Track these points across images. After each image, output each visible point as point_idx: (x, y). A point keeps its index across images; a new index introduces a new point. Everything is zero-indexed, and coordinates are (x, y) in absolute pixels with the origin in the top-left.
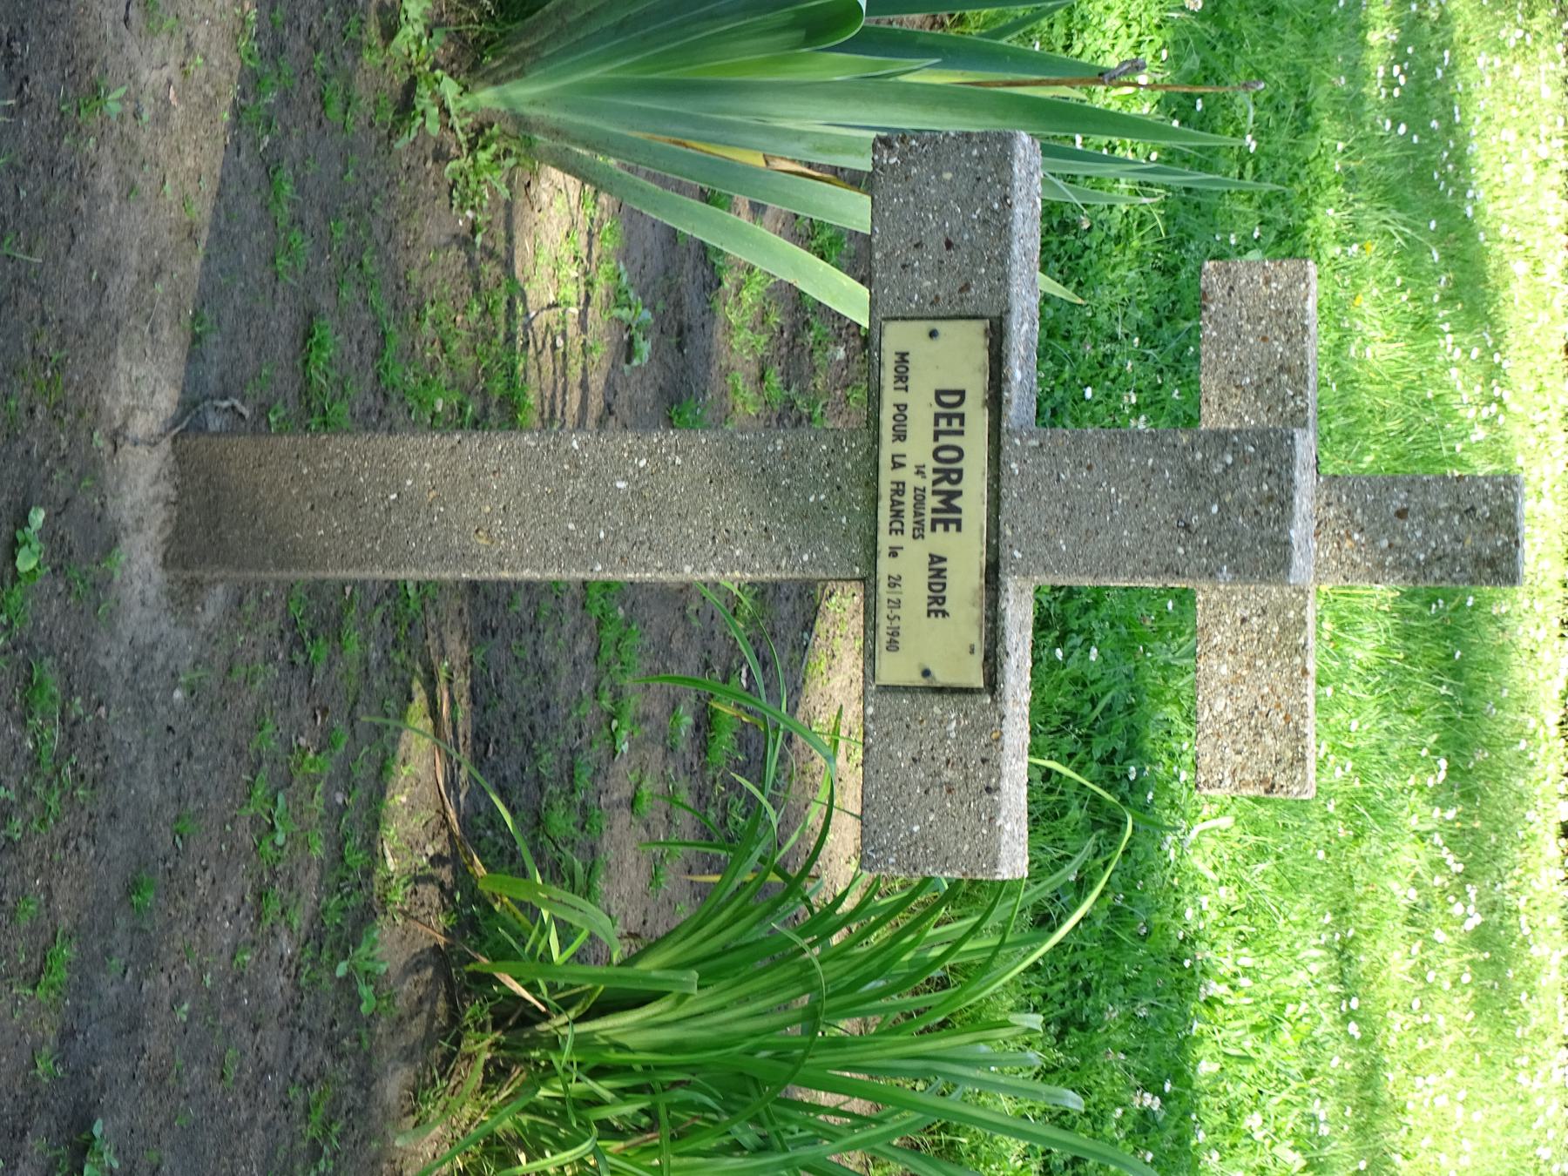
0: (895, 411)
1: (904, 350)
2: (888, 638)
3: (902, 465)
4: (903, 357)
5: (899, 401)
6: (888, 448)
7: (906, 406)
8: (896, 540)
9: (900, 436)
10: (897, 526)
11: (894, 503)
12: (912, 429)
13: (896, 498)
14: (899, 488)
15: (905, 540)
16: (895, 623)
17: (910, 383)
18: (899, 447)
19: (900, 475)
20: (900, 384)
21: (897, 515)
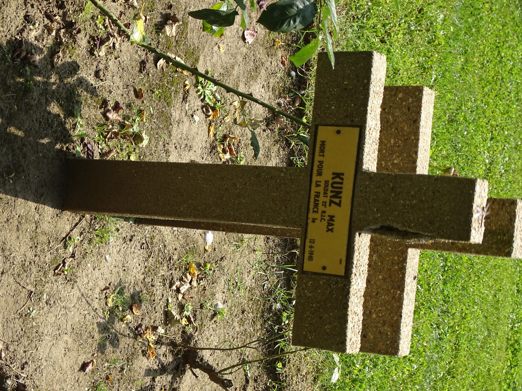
0: (318, 164)
1: (323, 140)
2: (309, 255)
3: (320, 186)
5: (320, 160)
6: (315, 178)
7: (323, 162)
8: (315, 216)
9: (320, 174)
10: (316, 209)
11: (316, 200)
12: (324, 171)
13: (316, 198)
14: (318, 195)
15: (318, 216)
16: (312, 250)
17: (326, 153)
18: (319, 178)
20: (321, 154)
21: (316, 205)
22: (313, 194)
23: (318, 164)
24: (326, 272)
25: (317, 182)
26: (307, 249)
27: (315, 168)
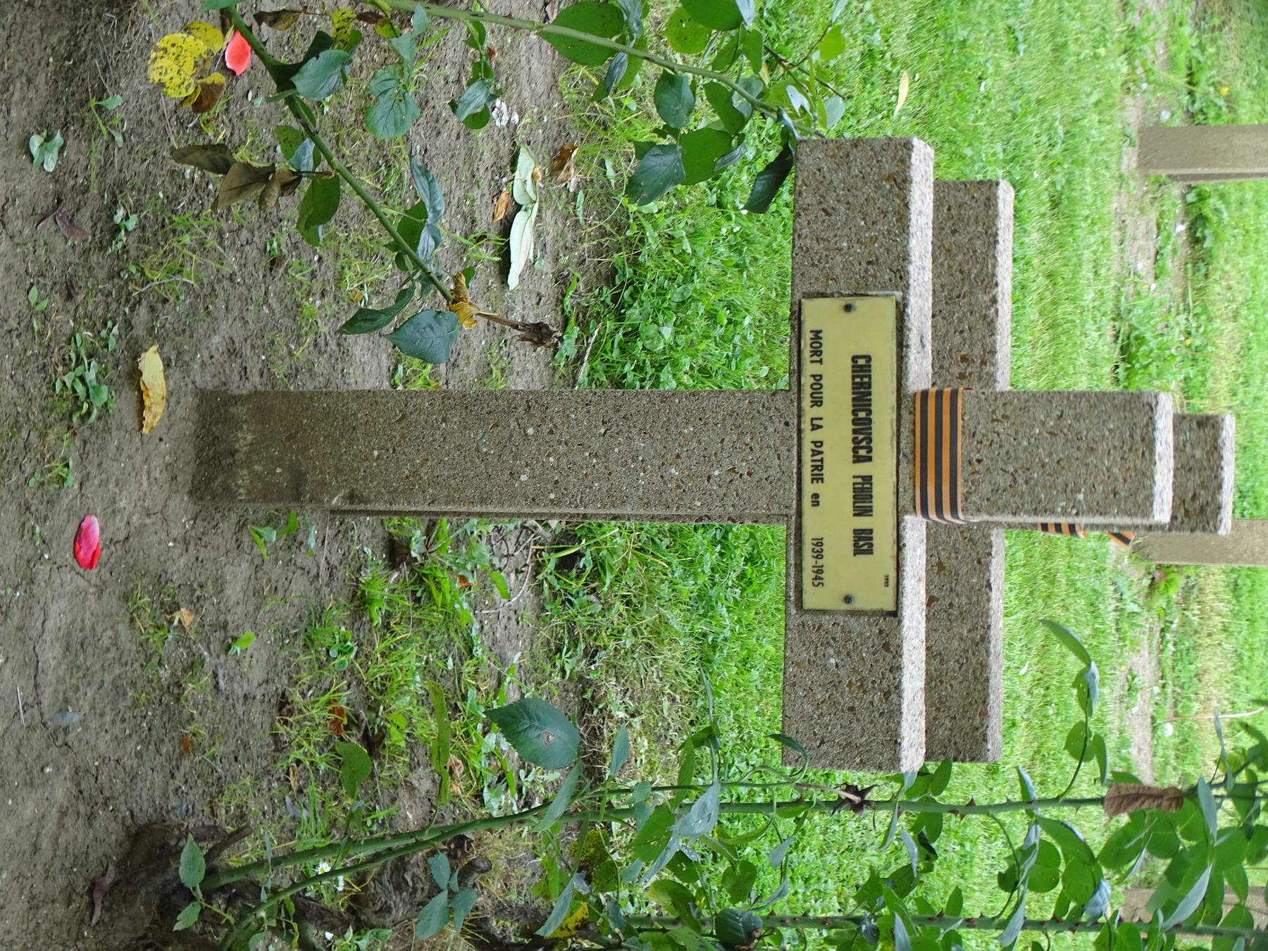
0: (812, 381)
2: (814, 575)
3: (820, 427)
4: (817, 334)
6: (810, 412)
9: (817, 402)
12: (827, 394)
16: (820, 562)
18: (816, 412)
19: (818, 435)
20: (815, 358)
21: (818, 466)
22: (808, 447)
23: (812, 381)
24: (858, 605)
25: (812, 419)
26: (808, 562)
27: (807, 391)
